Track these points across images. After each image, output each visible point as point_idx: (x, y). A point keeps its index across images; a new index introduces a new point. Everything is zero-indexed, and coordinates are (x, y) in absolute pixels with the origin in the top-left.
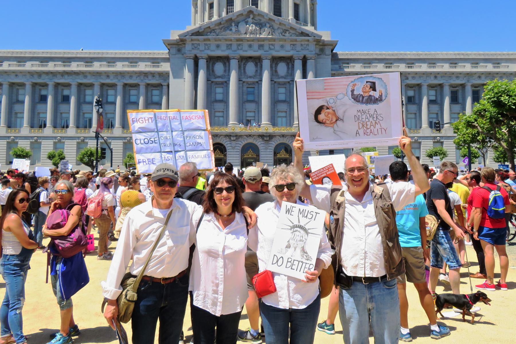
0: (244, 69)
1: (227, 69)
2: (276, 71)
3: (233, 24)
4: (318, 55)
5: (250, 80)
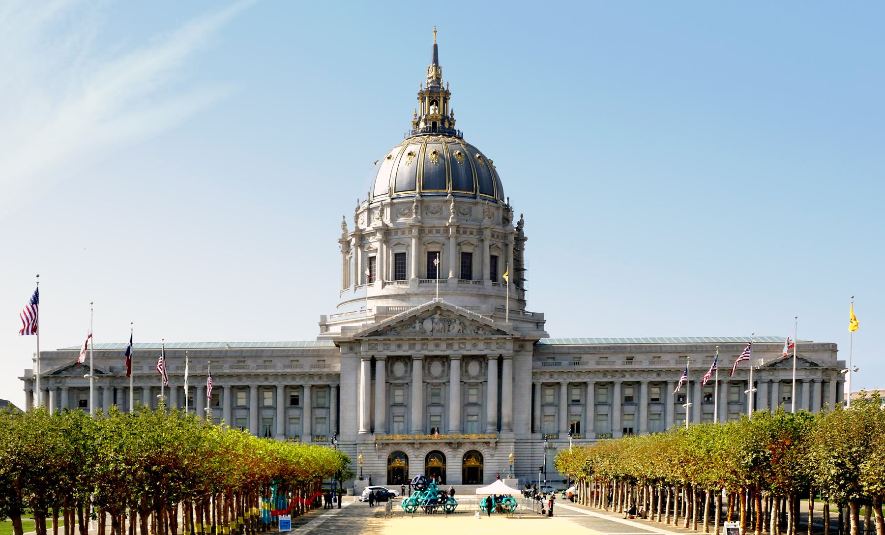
0: (429, 369)
1: (409, 369)
2: (467, 371)
3: (417, 321)
4: (517, 351)
5: (434, 381)
